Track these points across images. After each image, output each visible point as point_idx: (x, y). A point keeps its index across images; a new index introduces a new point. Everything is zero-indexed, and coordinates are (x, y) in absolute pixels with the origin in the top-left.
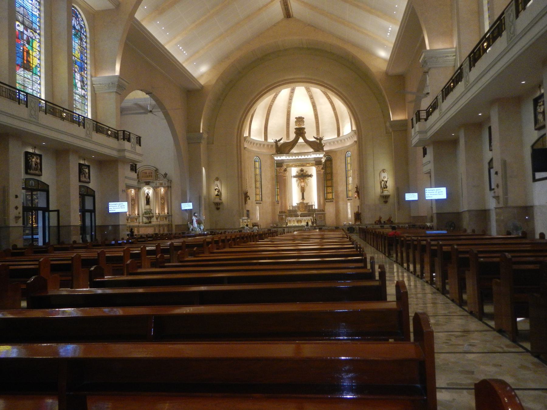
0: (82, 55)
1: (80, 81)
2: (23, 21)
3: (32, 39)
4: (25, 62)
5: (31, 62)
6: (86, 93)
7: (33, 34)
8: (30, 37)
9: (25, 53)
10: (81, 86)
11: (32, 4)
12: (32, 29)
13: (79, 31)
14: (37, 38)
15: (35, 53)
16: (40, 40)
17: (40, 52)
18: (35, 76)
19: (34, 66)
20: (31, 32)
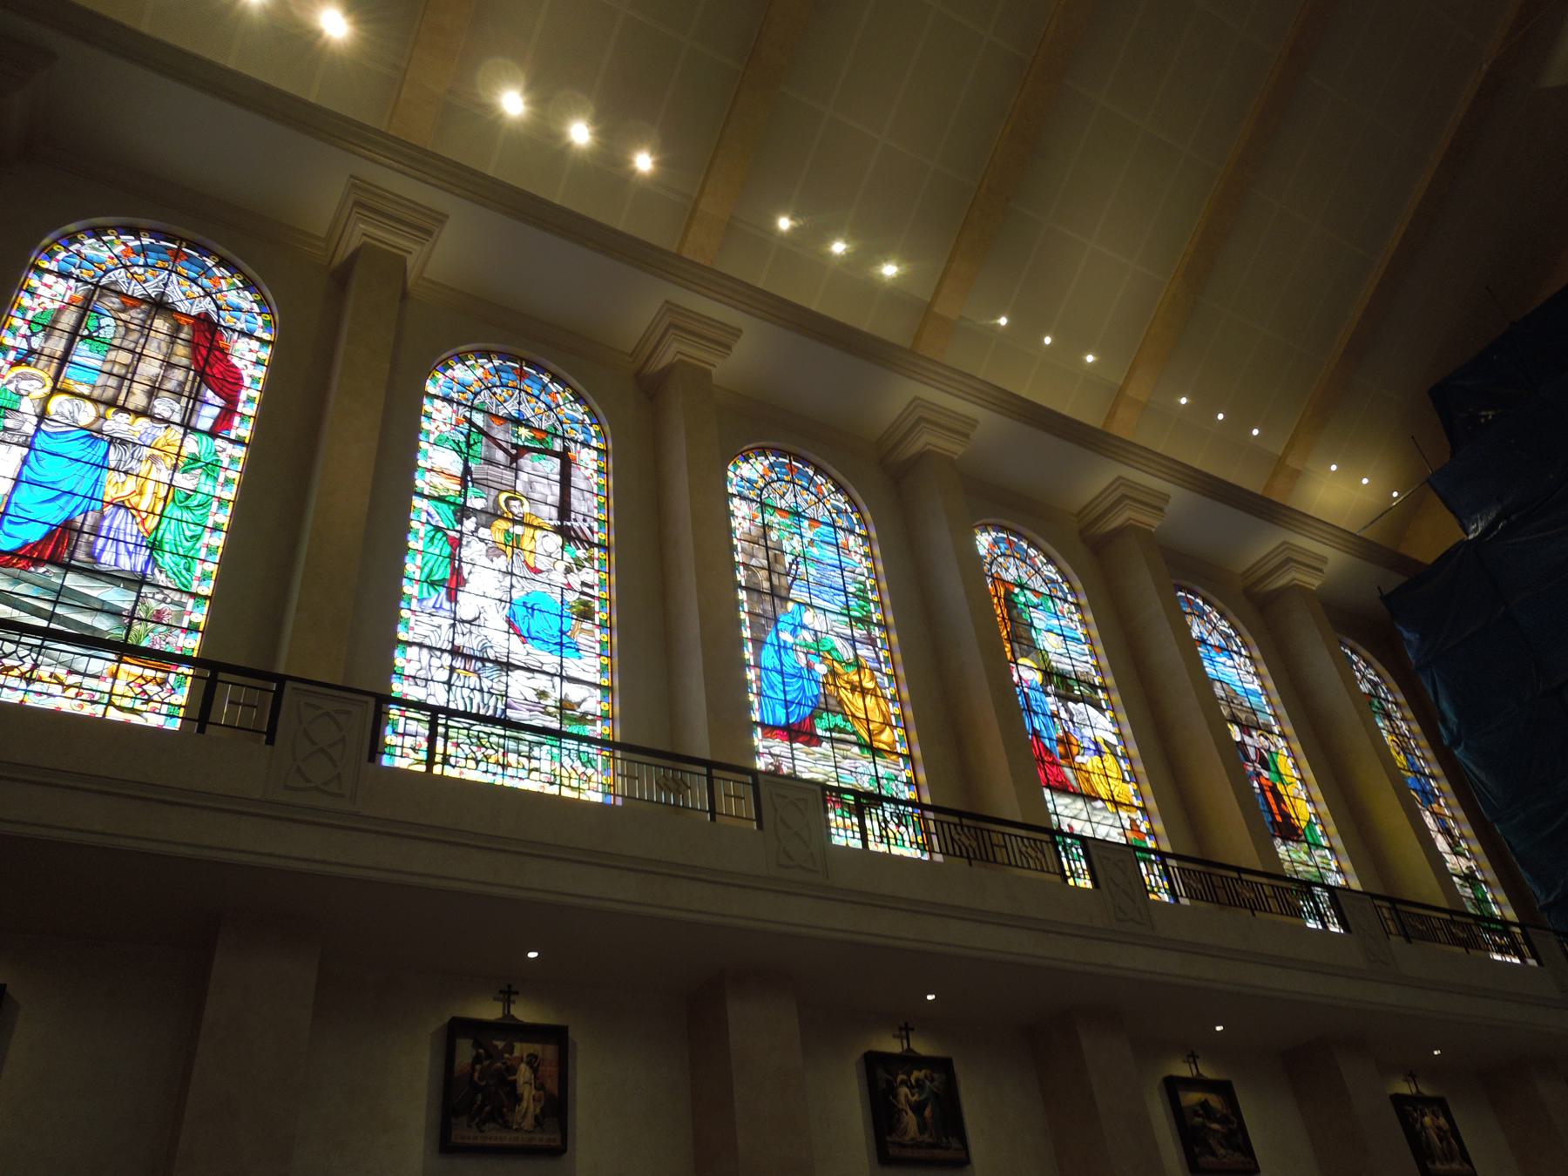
0: (1409, 757)
1: (1439, 831)
2: (1233, 715)
3: (1271, 752)
4: (1279, 818)
5: (1294, 816)
6: (1472, 864)
7: (1267, 738)
8: (1265, 750)
9: (1269, 795)
10: (1449, 845)
11: (1235, 667)
12: (1260, 729)
13: (1373, 696)
14: (1280, 747)
15: (1290, 786)
16: (1289, 748)
17: (1302, 780)
18: (1317, 853)
19: (1303, 824)
20: (1262, 735)
